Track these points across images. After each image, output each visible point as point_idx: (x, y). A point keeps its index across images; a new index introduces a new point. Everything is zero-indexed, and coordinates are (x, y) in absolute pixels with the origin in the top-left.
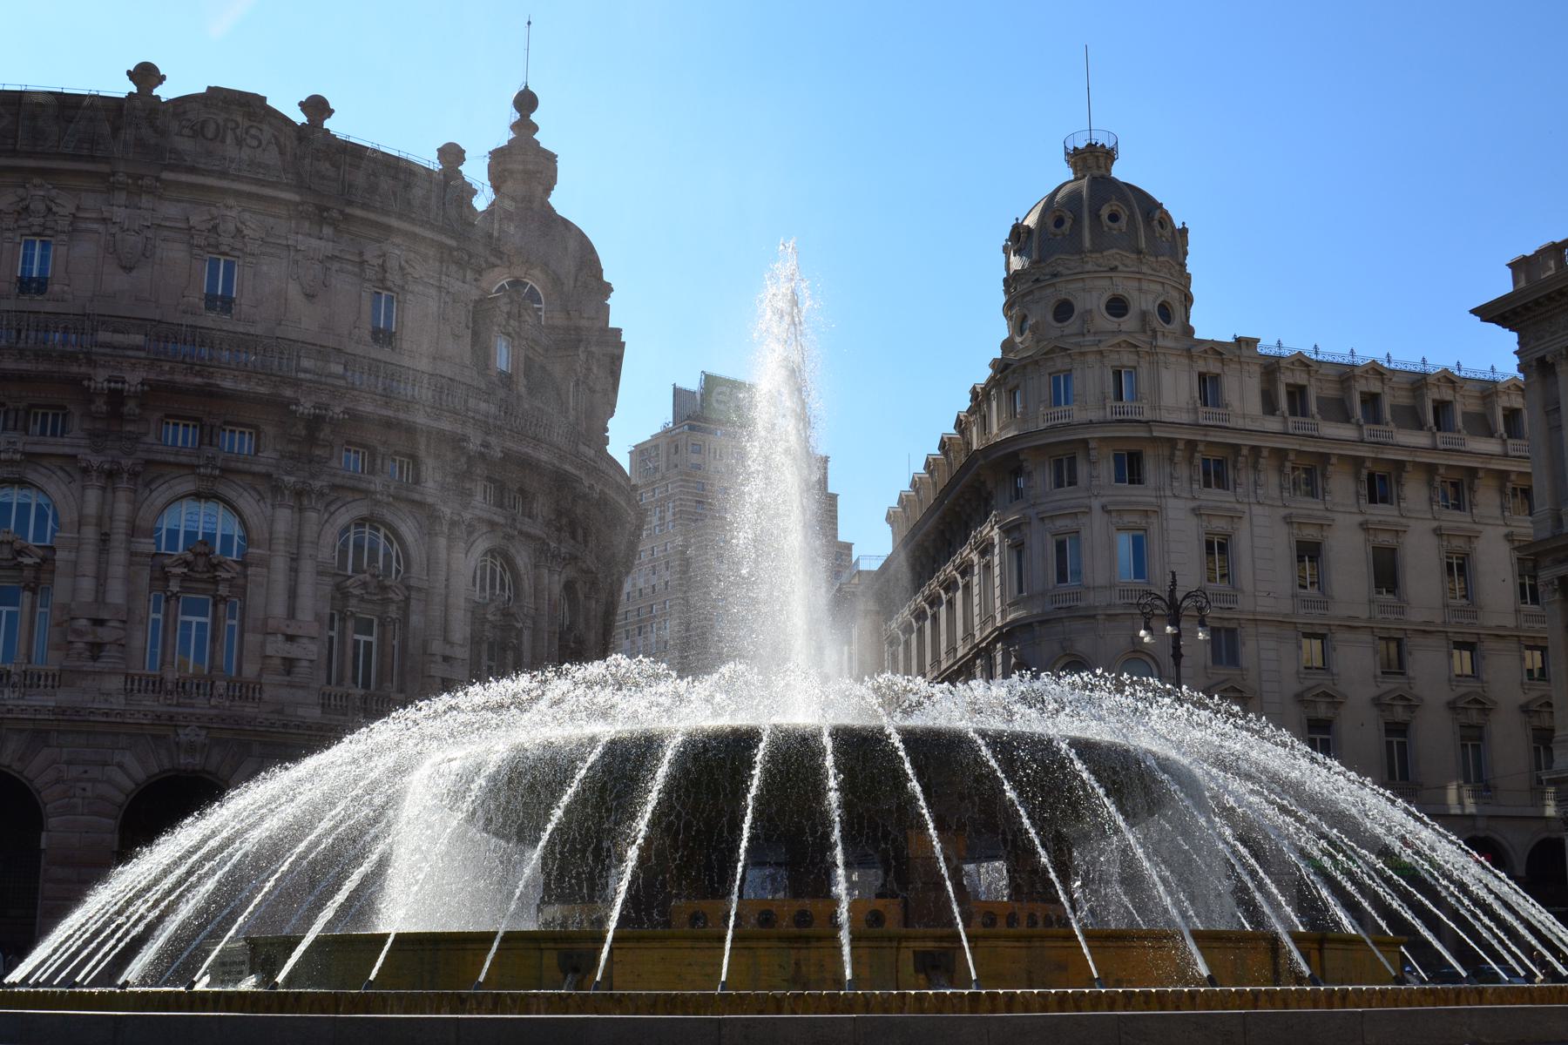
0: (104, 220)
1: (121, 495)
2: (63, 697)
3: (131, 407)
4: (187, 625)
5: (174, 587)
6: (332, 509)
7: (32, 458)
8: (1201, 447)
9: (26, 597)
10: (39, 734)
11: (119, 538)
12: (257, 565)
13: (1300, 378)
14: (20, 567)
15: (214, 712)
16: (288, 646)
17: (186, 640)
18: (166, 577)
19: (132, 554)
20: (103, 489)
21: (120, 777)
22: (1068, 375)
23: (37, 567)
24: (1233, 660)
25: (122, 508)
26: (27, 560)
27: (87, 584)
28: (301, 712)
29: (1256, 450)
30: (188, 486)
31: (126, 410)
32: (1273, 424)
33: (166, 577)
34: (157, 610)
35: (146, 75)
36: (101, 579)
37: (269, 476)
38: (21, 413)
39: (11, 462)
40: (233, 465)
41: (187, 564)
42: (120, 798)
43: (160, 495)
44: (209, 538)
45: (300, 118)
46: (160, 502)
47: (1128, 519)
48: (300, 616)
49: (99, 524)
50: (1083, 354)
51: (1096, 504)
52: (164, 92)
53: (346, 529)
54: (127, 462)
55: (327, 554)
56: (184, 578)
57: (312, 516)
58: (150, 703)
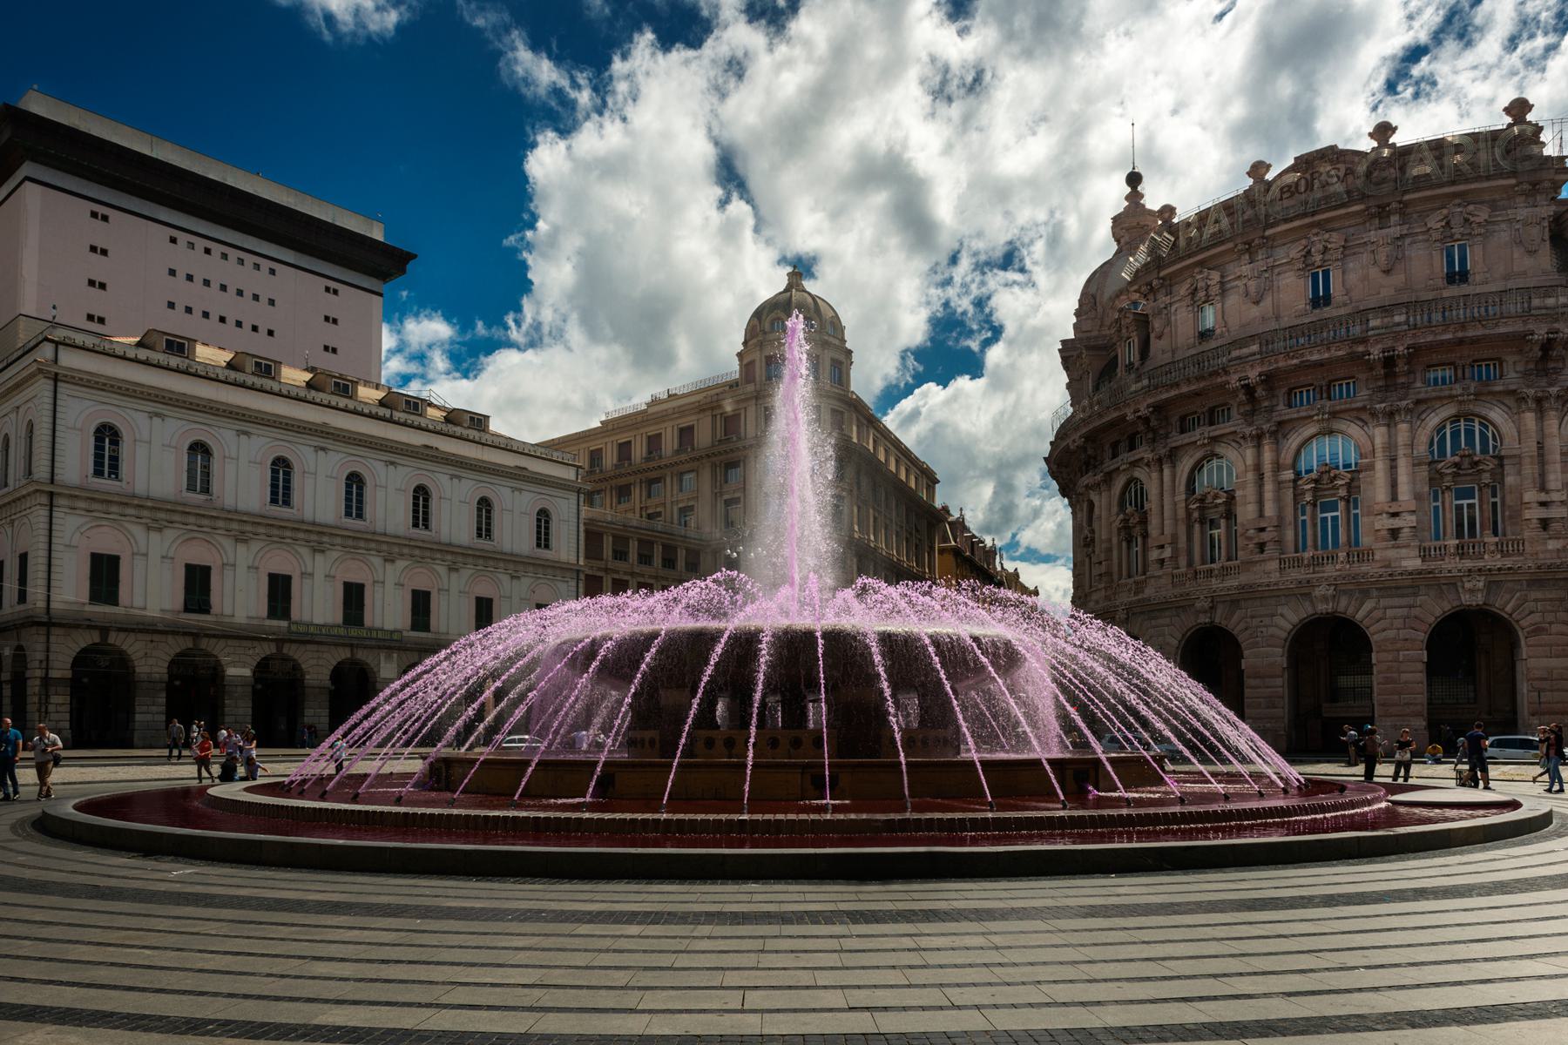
0: (1239, 277)
2: (1244, 578)
7: (1215, 440)
9: (1223, 522)
10: (1234, 603)
11: (1268, 475)
14: (1217, 506)
16: (1391, 520)
21: (1282, 622)
25: (1268, 456)
28: (1404, 563)
30: (1311, 429)
34: (1304, 514)
41: (1316, 481)
42: (1284, 635)
43: (1293, 442)
46: (1294, 446)
48: (1401, 498)
52: (1270, 176)
53: (1440, 429)
55: (1421, 449)
56: (1315, 490)
57: (1403, 427)
58: (1296, 574)
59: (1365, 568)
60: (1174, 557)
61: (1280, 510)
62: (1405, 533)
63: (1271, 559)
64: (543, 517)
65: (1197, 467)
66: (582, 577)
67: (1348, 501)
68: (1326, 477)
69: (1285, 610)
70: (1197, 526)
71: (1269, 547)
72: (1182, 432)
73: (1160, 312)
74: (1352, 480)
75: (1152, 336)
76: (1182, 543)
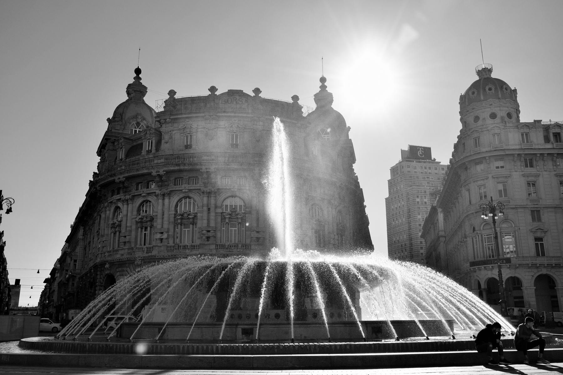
1: (212, 198)
4: (231, 230)
5: (227, 221)
8: (523, 156)
9: (191, 226)
11: (212, 209)
13: (557, 130)
14: (189, 218)
17: (231, 234)
18: (225, 218)
19: (216, 213)
20: (208, 197)
22: (479, 138)
23: (193, 218)
24: (539, 220)
26: (190, 217)
27: (205, 222)
29: (542, 155)
32: (549, 146)
33: (225, 218)
34: (224, 227)
35: (213, 89)
36: (208, 220)
39: (185, 192)
41: (230, 215)
45: (253, 94)
47: (500, 180)
49: (208, 206)
50: (482, 131)
51: (490, 176)
52: (217, 93)
56: (230, 218)
60: (167, 238)
61: (216, 223)
63: (213, 244)
65: (180, 200)
68: (234, 213)
70: (179, 226)
71: (212, 239)
72: (175, 185)
73: (168, 133)
75: (163, 141)
76: (171, 233)
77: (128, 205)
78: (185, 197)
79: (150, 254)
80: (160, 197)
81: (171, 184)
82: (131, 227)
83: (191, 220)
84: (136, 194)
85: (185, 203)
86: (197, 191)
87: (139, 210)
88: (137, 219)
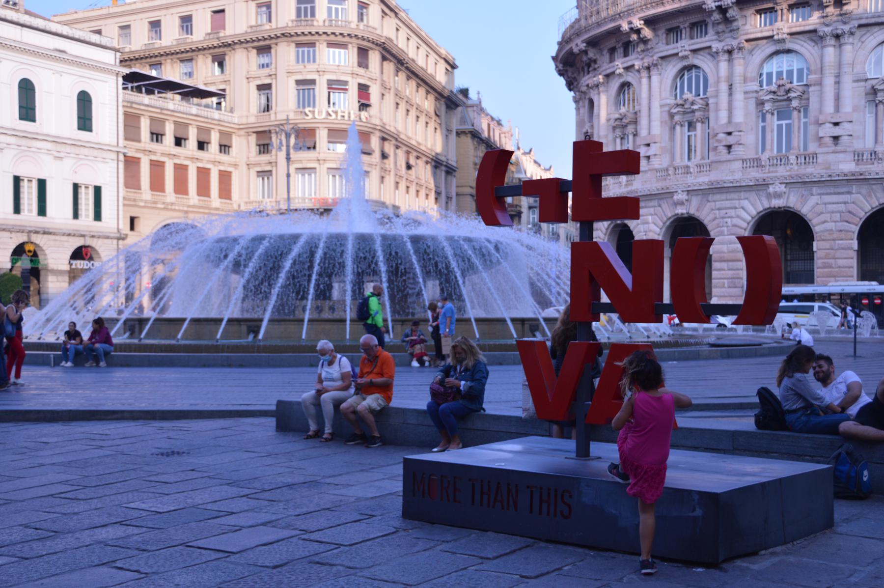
1: (736, 62)
3: (731, 13)
6: (863, 39)
12: (815, 85)
15: (788, 173)
19: (746, 93)
20: (730, 61)
26: (695, 107)
27: (723, 115)
30: (772, 48)
31: (728, 15)
37: (814, 31)
38: (688, 30)
40: (794, 30)
41: (774, 93)
44: (790, 73)
54: (735, 43)
57: (848, 48)
59: (810, 170)
61: (746, 115)
62: (844, 140)
64: (84, 100)
66: (121, 157)
67: (799, 111)
69: (746, 203)
72: (667, 44)
74: (804, 93)
77: (599, 94)
78: (689, 68)
79: (630, 188)
80: (644, 74)
81: (660, 44)
82: (606, 136)
83: (697, 114)
84: (609, 71)
85: (690, 80)
86: (707, 51)
87: (618, 103)
88: (612, 123)
